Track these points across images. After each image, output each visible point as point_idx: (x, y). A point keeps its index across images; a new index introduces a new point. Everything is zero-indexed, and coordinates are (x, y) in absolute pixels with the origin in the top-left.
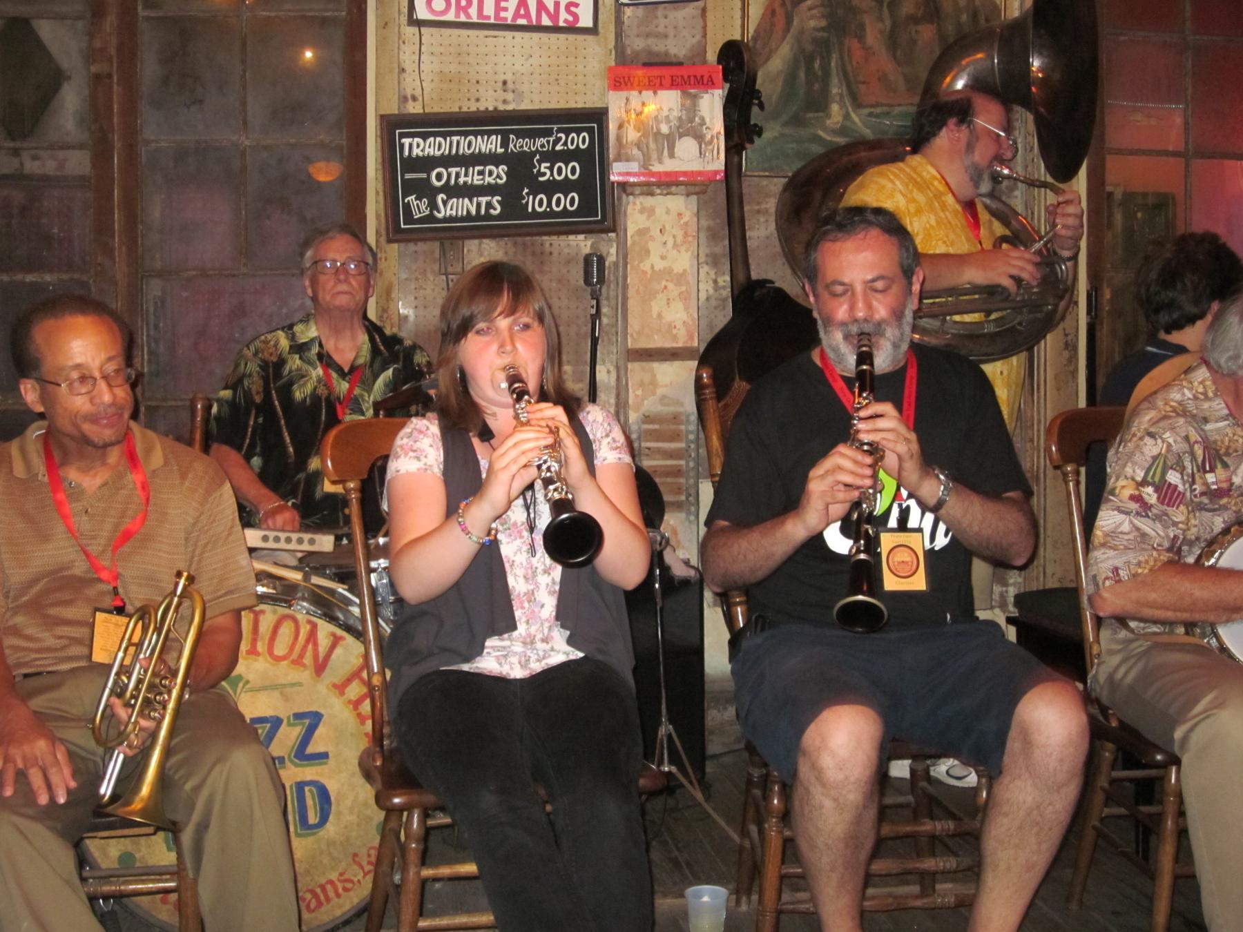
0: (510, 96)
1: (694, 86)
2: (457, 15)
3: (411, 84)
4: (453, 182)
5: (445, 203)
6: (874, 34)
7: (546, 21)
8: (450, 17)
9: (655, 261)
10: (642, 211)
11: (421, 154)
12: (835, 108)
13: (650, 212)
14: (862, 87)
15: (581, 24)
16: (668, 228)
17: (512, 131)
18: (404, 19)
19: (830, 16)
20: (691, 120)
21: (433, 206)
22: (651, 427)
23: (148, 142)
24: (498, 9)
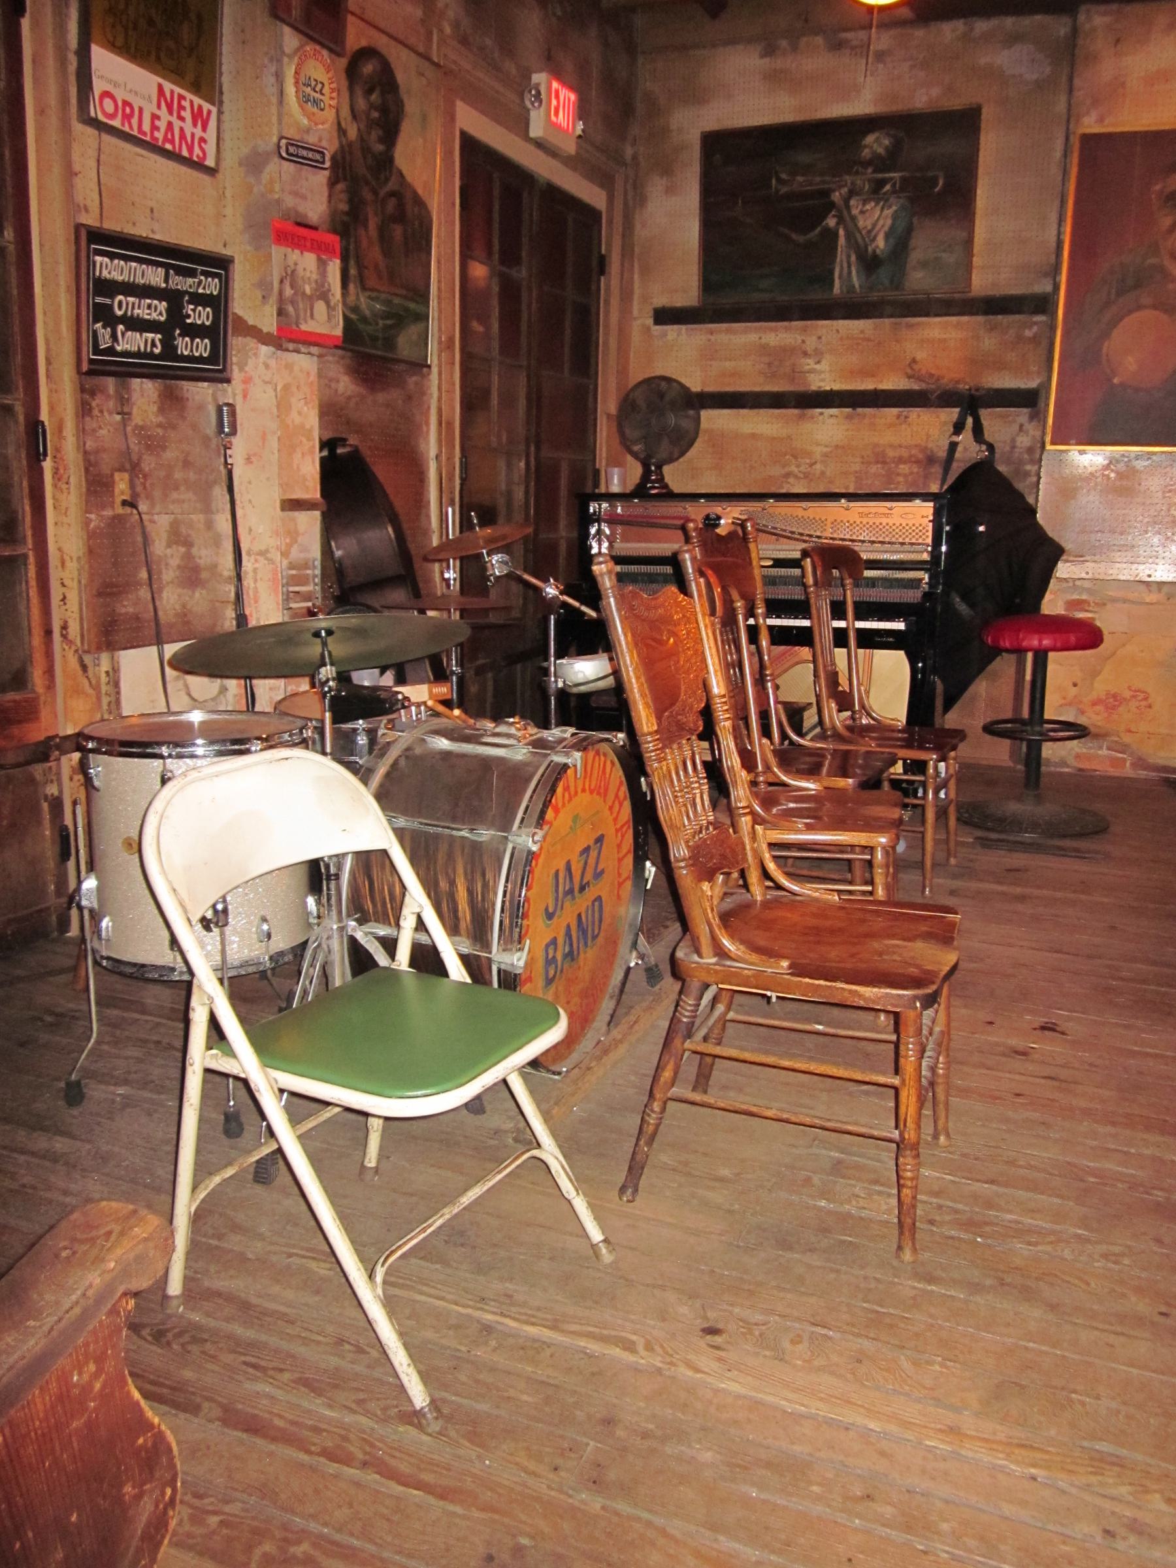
0: (156, 227)
2: (123, 125)
4: (129, 313)
5: (123, 334)
6: (373, 223)
7: (185, 153)
8: (116, 123)
11: (108, 276)
19: (350, 201)
20: (323, 286)
21: (114, 337)
22: (294, 572)
24: (154, 128)
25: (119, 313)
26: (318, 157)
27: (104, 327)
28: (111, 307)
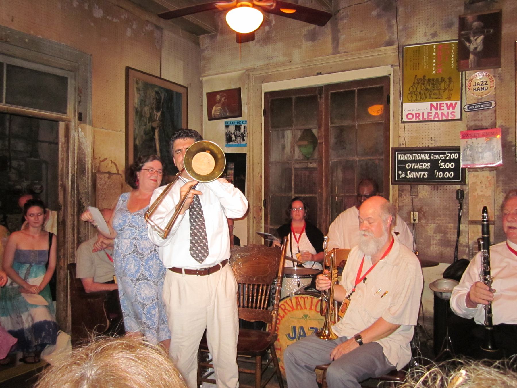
0: (433, 142)
1: (491, 136)
2: (416, 119)
3: (402, 141)
7: (444, 118)
8: (414, 120)
9: (479, 192)
10: (474, 176)
13: (477, 176)
15: (456, 118)
16: (483, 182)
17: (432, 153)
18: (400, 122)
23: (331, 160)
24: (429, 116)
26: (488, 105)
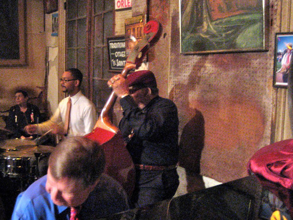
4: (119, 56)
5: (118, 61)
12: (205, 24)
14: (213, 12)
24: (129, 3)
25: (117, 56)
27: (114, 60)
28: (115, 55)
